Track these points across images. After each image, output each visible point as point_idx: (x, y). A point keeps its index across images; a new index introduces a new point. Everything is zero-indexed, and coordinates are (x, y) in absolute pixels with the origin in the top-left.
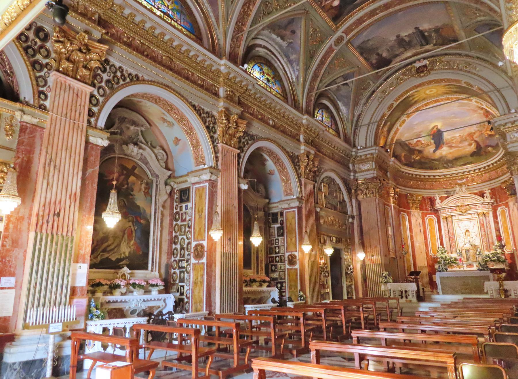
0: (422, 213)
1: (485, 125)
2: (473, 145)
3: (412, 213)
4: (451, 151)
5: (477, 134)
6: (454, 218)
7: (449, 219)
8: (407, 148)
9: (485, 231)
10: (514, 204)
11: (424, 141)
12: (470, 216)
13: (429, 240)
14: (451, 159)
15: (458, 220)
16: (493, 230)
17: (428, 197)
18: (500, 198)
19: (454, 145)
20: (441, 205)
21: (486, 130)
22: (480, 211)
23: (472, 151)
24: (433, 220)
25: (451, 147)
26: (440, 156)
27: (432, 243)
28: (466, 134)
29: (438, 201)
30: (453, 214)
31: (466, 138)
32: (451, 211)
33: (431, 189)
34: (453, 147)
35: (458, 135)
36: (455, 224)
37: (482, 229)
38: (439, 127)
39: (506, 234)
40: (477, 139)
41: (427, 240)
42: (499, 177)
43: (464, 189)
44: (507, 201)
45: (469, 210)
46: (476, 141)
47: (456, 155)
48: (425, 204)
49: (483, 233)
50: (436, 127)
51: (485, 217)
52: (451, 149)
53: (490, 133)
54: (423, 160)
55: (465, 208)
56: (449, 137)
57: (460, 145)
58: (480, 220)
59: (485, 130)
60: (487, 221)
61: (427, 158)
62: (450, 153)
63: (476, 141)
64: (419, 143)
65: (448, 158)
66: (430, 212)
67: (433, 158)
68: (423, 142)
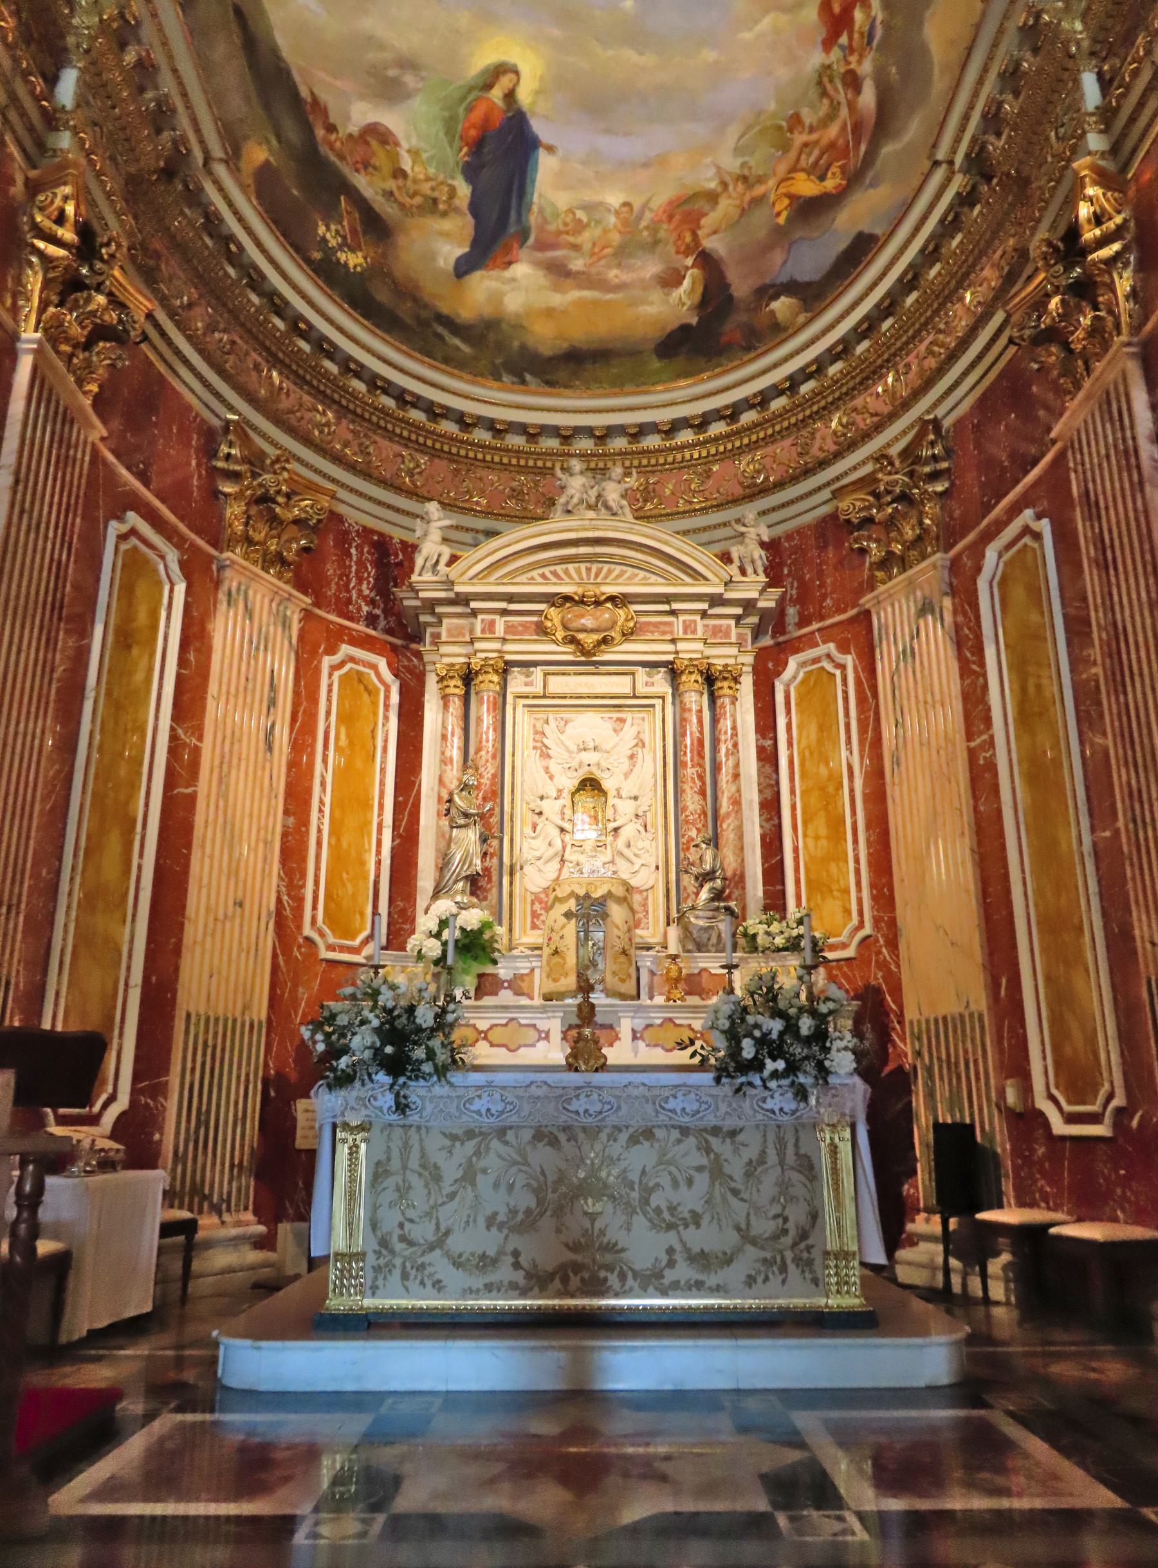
0: (307, 615)
1: (795, 121)
2: (686, 283)
3: (231, 580)
4: (557, 300)
5: (726, 206)
6: (517, 683)
7: (489, 683)
8: (293, 134)
9: (703, 793)
10: (926, 608)
11: (415, 153)
12: (619, 684)
13: (320, 821)
14: (546, 351)
15: (540, 702)
16: (751, 796)
17: (366, 532)
18: (801, 600)
19: (578, 264)
20: (454, 572)
21: (794, 169)
22: (690, 650)
23: (675, 325)
24: (371, 692)
25: (558, 272)
26: (488, 311)
27: (335, 849)
28: (660, 201)
29: (431, 547)
30: (516, 650)
31: (653, 228)
32: (509, 628)
33: (399, 489)
34: (568, 274)
35: (614, 199)
36: (521, 721)
37: (690, 771)
38: (525, 96)
39: (821, 826)
40: (712, 243)
41: (305, 822)
42: (823, 464)
43: (613, 493)
44: (866, 600)
45: (627, 635)
46: (706, 260)
47: (580, 333)
48: (344, 575)
49: (692, 802)
50: (506, 82)
51: (713, 699)
52: (556, 288)
53: (807, 187)
54: (382, 295)
55: (607, 613)
56: (562, 200)
57: (613, 274)
58: (682, 710)
59: (782, 169)
60: (726, 724)
61: (407, 291)
62: (550, 312)
63: (706, 260)
64: (380, 159)
65: (531, 342)
66: (361, 627)
67: (445, 308)
68: (407, 164)
